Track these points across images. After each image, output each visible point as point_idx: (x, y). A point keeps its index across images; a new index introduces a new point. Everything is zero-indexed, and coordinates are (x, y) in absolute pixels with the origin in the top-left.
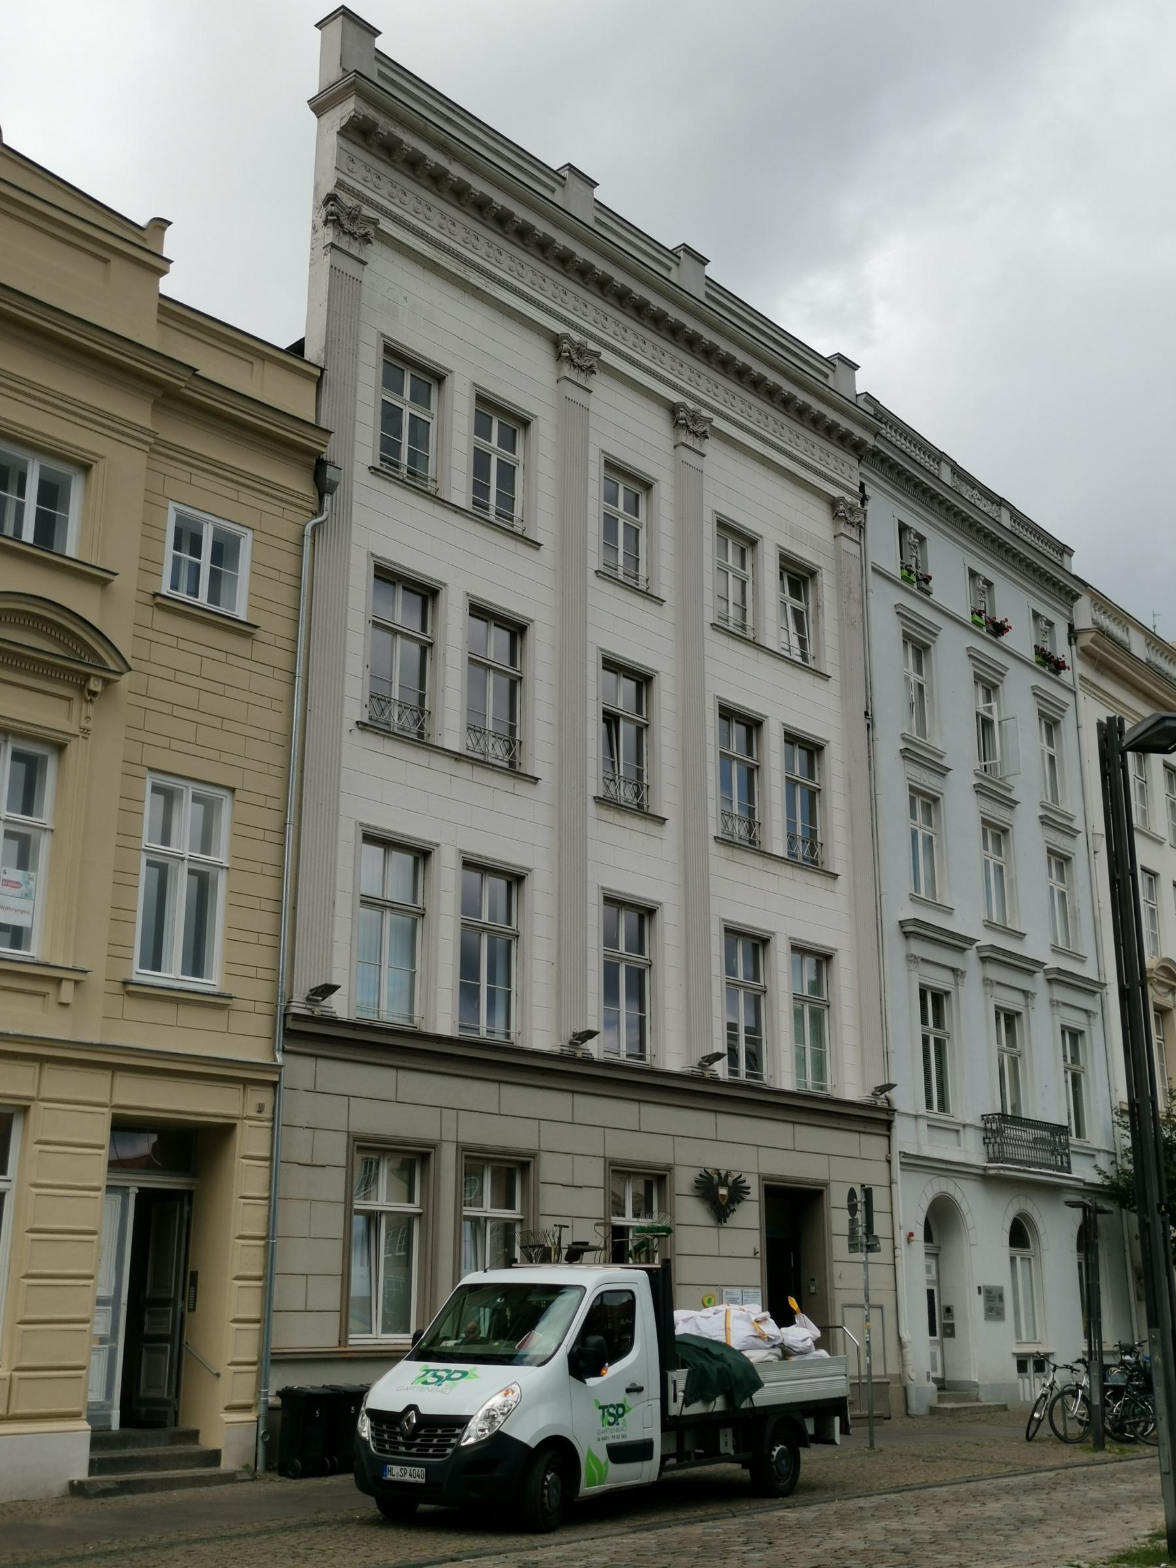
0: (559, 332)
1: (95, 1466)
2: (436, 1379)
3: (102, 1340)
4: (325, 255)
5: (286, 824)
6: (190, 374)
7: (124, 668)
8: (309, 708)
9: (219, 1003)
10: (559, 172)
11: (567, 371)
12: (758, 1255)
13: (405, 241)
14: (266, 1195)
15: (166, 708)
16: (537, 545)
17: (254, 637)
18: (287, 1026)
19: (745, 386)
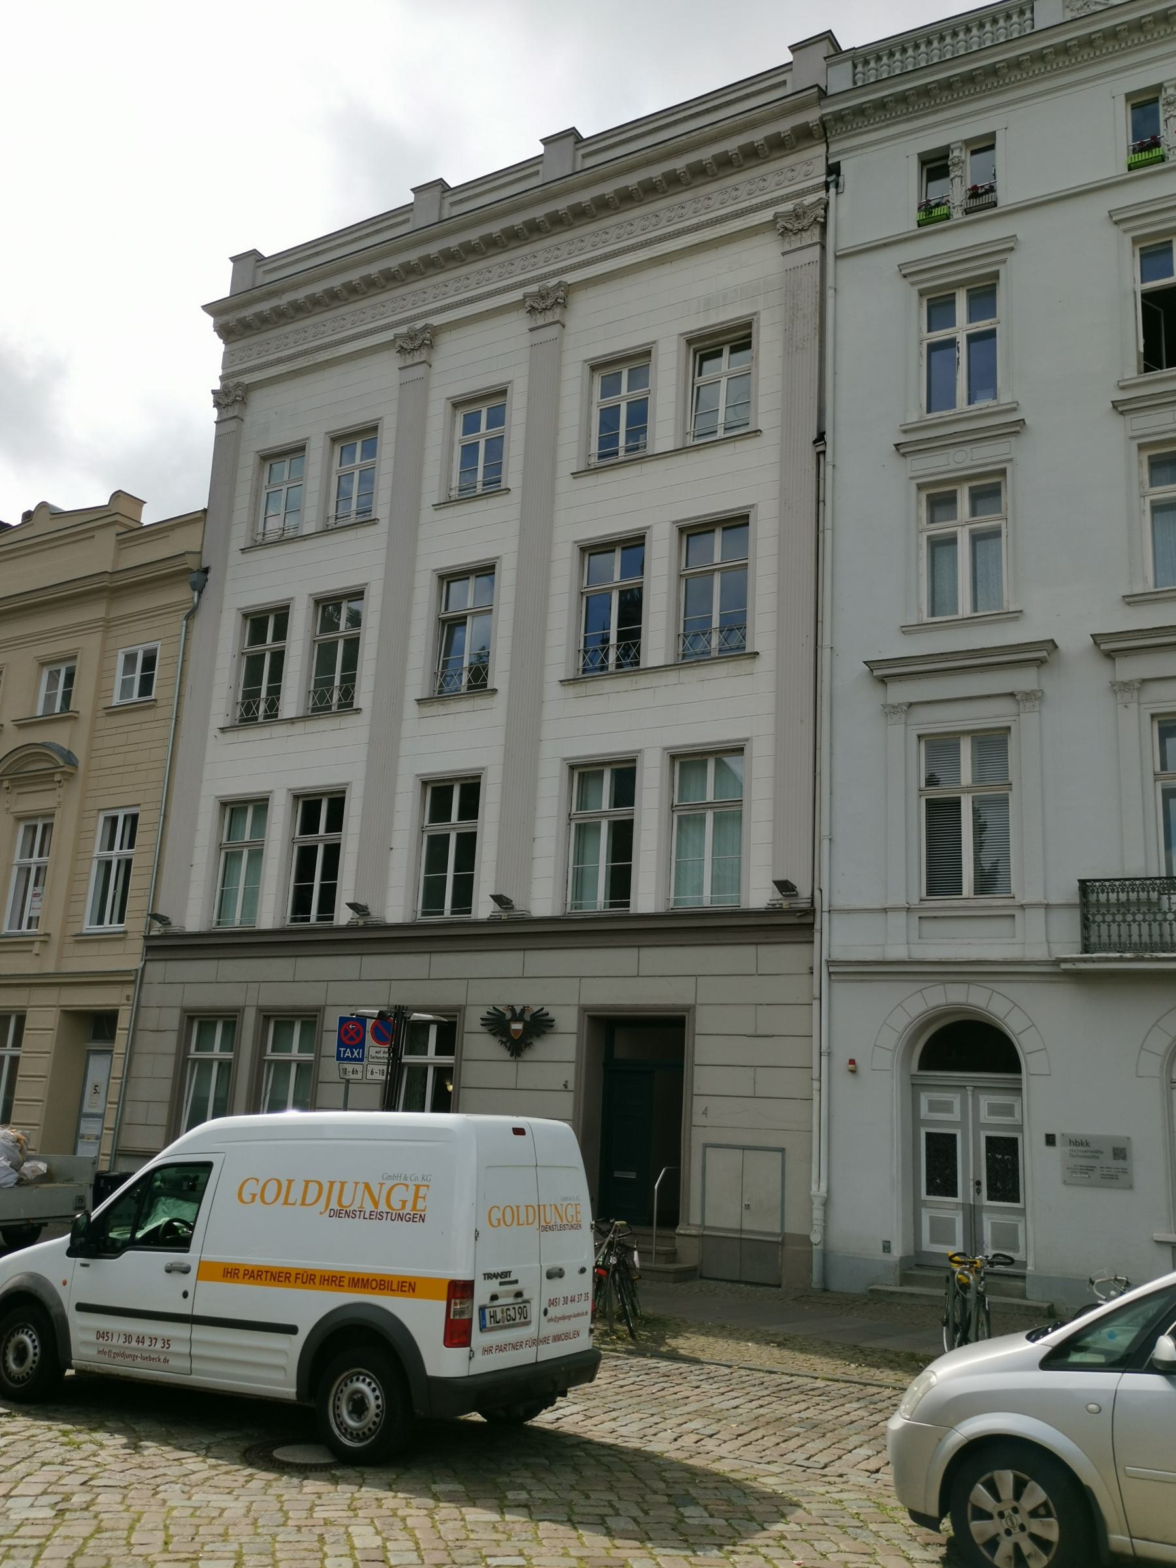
12: (571, 1086)
19: (576, 224)
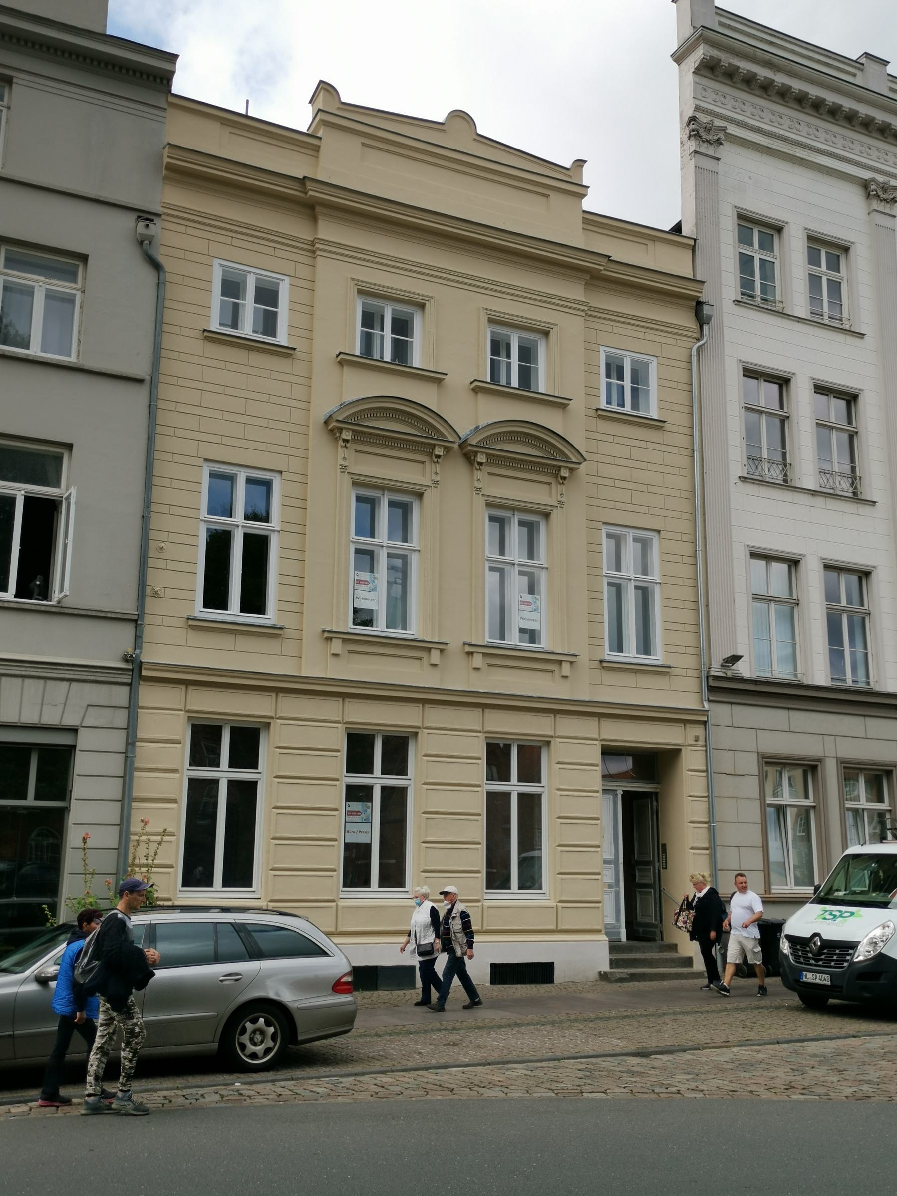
0: (866, 178)
1: (613, 963)
2: (832, 917)
3: (610, 886)
4: (691, 160)
5: (696, 551)
6: (606, 260)
7: (581, 460)
8: (705, 472)
9: (662, 671)
10: (858, 61)
11: (875, 205)
13: (747, 137)
14: (706, 795)
15: (611, 483)
16: (861, 336)
17: (664, 428)
18: (709, 685)
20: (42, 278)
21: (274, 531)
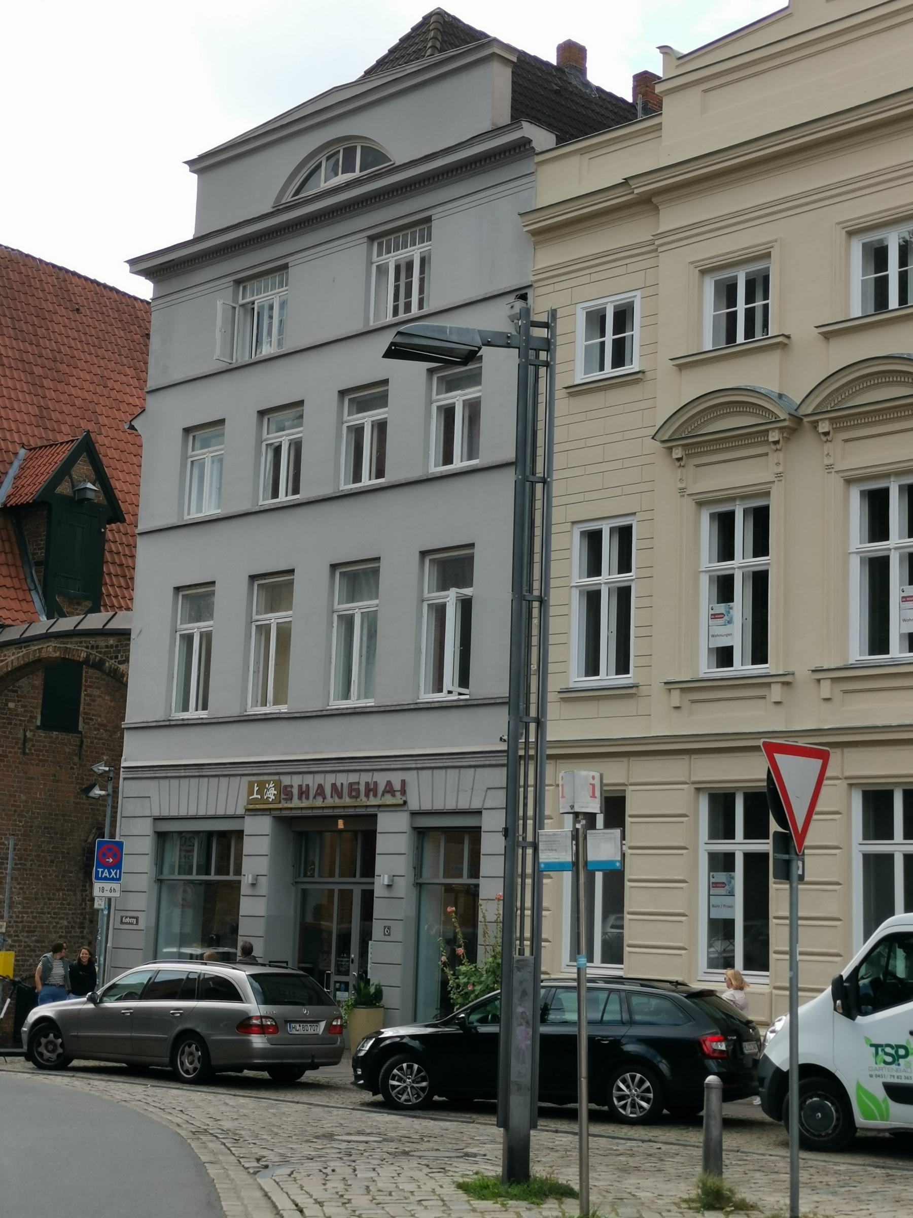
20: (459, 392)
21: (632, 580)
